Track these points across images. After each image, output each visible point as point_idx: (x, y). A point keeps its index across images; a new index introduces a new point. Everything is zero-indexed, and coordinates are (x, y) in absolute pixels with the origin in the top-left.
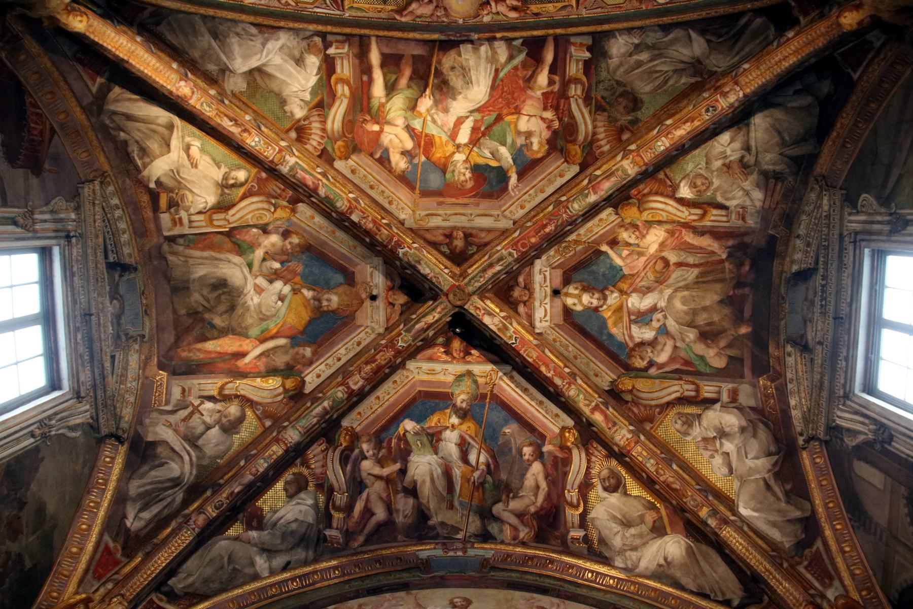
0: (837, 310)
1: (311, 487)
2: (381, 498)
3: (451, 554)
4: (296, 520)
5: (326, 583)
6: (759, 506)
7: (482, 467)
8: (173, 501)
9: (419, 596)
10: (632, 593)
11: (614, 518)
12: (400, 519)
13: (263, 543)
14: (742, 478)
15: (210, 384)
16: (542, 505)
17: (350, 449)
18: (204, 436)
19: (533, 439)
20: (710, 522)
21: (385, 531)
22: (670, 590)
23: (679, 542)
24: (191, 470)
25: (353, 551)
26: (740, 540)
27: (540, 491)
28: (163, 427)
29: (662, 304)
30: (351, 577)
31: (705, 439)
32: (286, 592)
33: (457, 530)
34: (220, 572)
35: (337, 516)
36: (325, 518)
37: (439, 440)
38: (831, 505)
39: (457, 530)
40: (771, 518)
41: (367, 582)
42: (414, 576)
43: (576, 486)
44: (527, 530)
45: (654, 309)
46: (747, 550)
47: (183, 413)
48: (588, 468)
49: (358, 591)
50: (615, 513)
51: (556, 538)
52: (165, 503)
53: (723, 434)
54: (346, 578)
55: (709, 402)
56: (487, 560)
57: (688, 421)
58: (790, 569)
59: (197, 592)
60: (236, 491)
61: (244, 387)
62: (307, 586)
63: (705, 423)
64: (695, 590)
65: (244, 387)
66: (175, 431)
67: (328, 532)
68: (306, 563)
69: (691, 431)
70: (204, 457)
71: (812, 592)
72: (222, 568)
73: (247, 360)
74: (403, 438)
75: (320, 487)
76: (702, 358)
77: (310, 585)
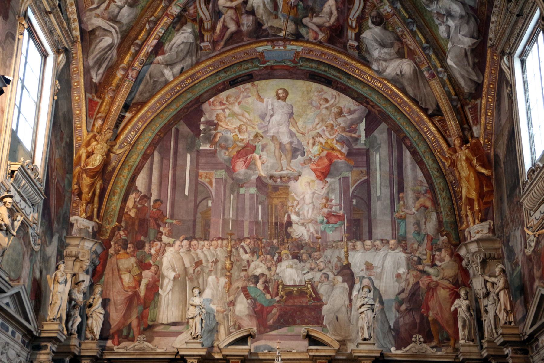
0: (522, 10)
1: (189, 23)
2: (232, 19)
3: (277, 48)
4: (183, 43)
5: (205, 76)
6: (458, 63)
8: (112, 56)
9: (259, 87)
10: (379, 88)
11: (376, 40)
12: (245, 28)
13: (166, 62)
14: (453, 43)
16: (333, 23)
18: (120, 14)
20: (425, 73)
21: (236, 37)
22: (399, 93)
23: (410, 65)
24: (118, 36)
25: (218, 52)
26: (438, 91)
27: (333, 16)
28: (95, 19)
30: (219, 69)
31: (438, 13)
32: (185, 87)
33: (280, 30)
34: (147, 86)
35: (207, 36)
36: (199, 37)
38: (491, 86)
39: (280, 30)
40: (463, 73)
41: (228, 73)
42: (255, 67)
43: (355, 17)
44: (323, 35)
46: (440, 96)
47: (104, 6)
48: (364, 8)
49: (224, 82)
50: (377, 38)
51: (340, 43)
52: (108, 60)
53: (449, 14)
54: (216, 71)
56: (298, 52)
58: (460, 109)
59: (139, 101)
60: (149, 51)
62: (195, 80)
63: (440, 4)
64: (412, 96)
66: (103, 18)
67: (202, 45)
68: (192, 66)
69: (431, 6)
70: (123, 26)
71: (466, 126)
72: (148, 83)
75: (194, 20)
77: (197, 79)
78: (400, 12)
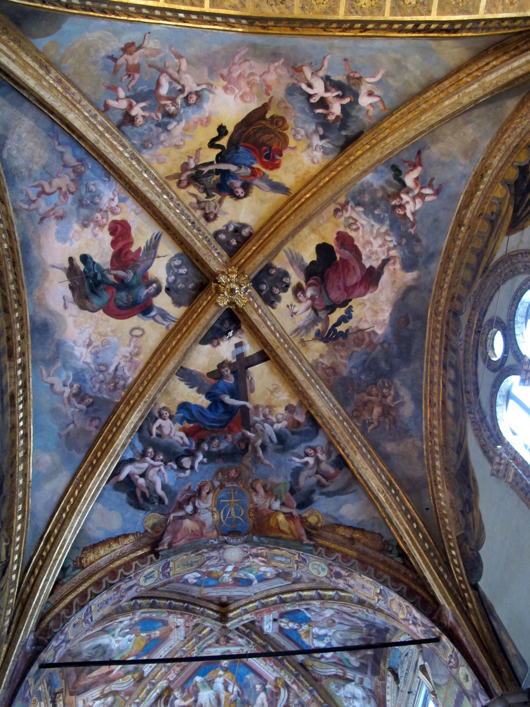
7: (235, 693)
15: (96, 692)
17: (169, 696)
19: (261, 681)
29: (330, 634)
31: (346, 697)
37: (213, 683)
45: (326, 635)
48: (288, 698)
53: (354, 697)
55: (350, 681)
57: (338, 687)
61: (114, 687)
63: (346, 689)
65: (114, 687)
73: (114, 673)
74: (195, 685)
76: (348, 660)
78: (317, 699)
